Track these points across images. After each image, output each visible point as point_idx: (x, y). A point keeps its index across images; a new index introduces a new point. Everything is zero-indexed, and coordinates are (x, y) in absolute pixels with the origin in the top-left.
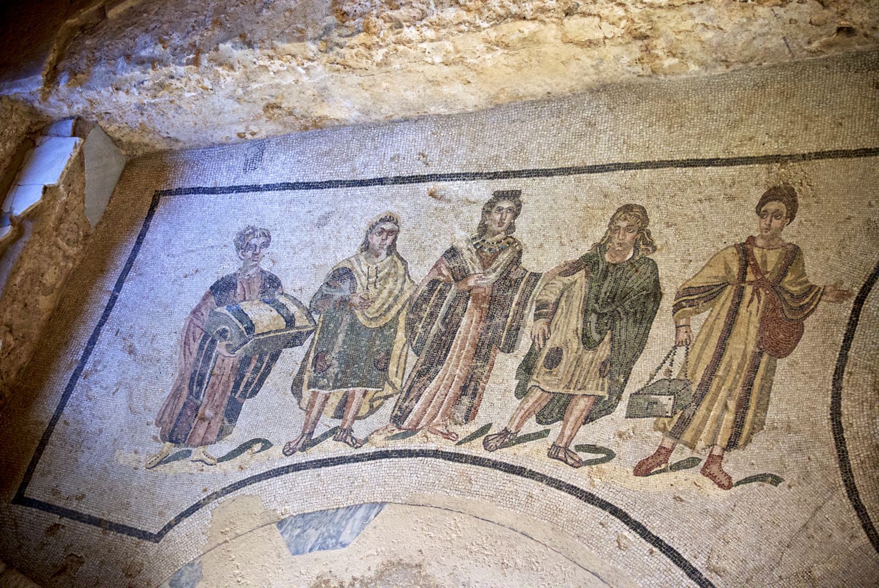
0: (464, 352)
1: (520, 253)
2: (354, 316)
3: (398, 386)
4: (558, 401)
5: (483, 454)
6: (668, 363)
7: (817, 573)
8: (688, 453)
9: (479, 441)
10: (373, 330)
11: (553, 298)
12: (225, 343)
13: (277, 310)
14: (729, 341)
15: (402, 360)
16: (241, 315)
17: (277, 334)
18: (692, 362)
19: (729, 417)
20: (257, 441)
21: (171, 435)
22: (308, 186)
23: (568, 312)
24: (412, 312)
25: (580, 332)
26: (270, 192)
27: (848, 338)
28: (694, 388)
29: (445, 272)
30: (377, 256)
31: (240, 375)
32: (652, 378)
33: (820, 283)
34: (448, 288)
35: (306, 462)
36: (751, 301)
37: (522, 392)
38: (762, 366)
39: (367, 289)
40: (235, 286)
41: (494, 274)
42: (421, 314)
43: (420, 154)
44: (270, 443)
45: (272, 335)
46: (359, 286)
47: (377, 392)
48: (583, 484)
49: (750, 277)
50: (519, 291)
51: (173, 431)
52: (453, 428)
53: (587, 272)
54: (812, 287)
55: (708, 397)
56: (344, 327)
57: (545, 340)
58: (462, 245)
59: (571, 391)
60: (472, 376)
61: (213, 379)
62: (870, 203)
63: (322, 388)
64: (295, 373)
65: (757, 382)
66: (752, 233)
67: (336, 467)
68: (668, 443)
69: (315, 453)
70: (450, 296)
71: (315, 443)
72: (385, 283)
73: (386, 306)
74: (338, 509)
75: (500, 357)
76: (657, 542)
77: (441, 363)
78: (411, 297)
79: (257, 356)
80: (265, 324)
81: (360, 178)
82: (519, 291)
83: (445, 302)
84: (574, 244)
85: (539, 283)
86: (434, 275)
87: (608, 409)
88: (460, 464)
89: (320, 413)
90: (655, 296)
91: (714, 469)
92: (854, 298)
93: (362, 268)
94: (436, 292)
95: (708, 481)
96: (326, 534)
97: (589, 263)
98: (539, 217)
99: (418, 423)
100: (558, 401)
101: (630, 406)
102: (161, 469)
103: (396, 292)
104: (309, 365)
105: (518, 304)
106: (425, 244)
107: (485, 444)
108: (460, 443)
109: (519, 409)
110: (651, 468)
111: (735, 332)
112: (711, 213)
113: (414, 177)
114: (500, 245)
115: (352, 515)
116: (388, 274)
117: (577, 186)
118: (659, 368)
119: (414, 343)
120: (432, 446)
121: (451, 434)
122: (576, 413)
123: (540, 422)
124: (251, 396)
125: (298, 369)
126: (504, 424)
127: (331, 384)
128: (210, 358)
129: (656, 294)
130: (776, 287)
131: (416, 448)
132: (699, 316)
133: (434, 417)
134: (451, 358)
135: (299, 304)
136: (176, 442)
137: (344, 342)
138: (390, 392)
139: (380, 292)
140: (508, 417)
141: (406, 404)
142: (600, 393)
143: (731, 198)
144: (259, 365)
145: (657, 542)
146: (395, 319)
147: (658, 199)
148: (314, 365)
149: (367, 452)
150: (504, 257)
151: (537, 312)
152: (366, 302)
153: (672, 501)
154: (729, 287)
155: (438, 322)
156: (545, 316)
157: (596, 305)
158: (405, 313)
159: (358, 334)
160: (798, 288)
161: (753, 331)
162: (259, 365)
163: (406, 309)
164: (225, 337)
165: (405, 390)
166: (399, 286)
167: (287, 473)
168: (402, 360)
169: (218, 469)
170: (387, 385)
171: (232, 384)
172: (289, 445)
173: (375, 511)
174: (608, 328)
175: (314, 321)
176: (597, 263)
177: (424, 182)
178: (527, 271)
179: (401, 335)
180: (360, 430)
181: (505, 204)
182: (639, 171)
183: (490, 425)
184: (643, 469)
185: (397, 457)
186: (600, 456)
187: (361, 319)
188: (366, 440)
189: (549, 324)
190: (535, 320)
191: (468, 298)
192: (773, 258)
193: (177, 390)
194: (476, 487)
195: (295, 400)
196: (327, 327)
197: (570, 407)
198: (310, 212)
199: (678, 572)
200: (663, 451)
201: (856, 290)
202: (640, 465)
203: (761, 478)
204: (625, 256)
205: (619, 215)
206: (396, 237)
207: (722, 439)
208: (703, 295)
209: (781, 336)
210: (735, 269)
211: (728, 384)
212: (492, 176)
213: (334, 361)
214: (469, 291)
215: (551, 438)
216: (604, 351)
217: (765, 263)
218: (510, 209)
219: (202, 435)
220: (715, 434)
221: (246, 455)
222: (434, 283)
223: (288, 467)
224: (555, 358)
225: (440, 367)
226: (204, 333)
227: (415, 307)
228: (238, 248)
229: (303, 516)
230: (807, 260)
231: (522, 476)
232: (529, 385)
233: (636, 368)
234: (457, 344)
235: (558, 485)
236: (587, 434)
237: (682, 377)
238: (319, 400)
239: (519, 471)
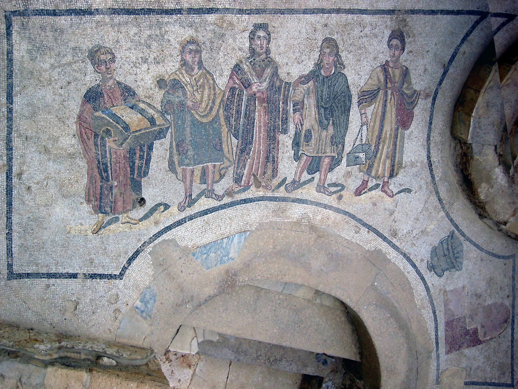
0: (262, 135)
1: (277, 68)
2: (192, 115)
3: (232, 160)
4: (315, 161)
5: (287, 195)
6: (360, 136)
8: (375, 182)
9: (282, 188)
12: (112, 139)
13: (141, 114)
16: (114, 116)
17: (146, 131)
20: (160, 204)
28: (373, 148)
30: (193, 70)
34: (242, 93)
35: (194, 214)
36: (391, 99)
37: (297, 158)
39: (194, 94)
40: (101, 95)
41: (265, 83)
44: (168, 205)
45: (143, 132)
46: (188, 93)
47: (221, 165)
49: (389, 85)
53: (314, 82)
55: (380, 152)
57: (302, 125)
60: (270, 150)
63: (188, 165)
64: (168, 157)
65: (398, 143)
67: (212, 214)
69: (197, 208)
74: (222, 239)
75: (281, 137)
79: (139, 148)
82: (282, 94)
83: (243, 103)
85: (291, 89)
86: (231, 84)
88: (277, 203)
89: (191, 182)
91: (386, 188)
92: (432, 97)
94: (236, 96)
96: (221, 255)
97: (313, 75)
99: (249, 182)
100: (315, 161)
101: (347, 160)
103: (212, 97)
104: (175, 151)
108: (273, 191)
109: (298, 167)
110: (361, 191)
115: (232, 242)
116: (203, 83)
118: (357, 138)
120: (261, 194)
122: (325, 166)
123: (309, 174)
124: (145, 176)
125: (168, 154)
127: (192, 163)
131: (252, 197)
134: (256, 140)
135: (154, 108)
137: (191, 133)
139: (202, 97)
140: (294, 173)
142: (333, 154)
144: (142, 153)
146: (217, 115)
149: (227, 202)
150: (268, 71)
151: (294, 108)
152: (197, 105)
154: (381, 91)
156: (299, 110)
157: (322, 103)
158: (222, 111)
161: (394, 116)
162: (142, 153)
164: (110, 135)
165: (236, 162)
167: (186, 222)
168: (229, 141)
170: (225, 160)
171: (129, 169)
172: (180, 205)
174: (330, 116)
175: (168, 120)
176: (318, 76)
178: (283, 81)
183: (286, 178)
184: (358, 192)
185: (244, 204)
186: (339, 188)
187: (197, 117)
189: (301, 115)
190: (294, 113)
197: (321, 163)
202: (357, 190)
204: (331, 72)
208: (370, 96)
209: (405, 119)
214: (255, 95)
215: (316, 181)
216: (331, 130)
222: (233, 89)
223: (185, 218)
224: (308, 136)
225: (251, 146)
226: (93, 133)
231: (307, 204)
232: (301, 152)
234: (256, 130)
235: (326, 207)
236: (332, 177)
237: (367, 143)
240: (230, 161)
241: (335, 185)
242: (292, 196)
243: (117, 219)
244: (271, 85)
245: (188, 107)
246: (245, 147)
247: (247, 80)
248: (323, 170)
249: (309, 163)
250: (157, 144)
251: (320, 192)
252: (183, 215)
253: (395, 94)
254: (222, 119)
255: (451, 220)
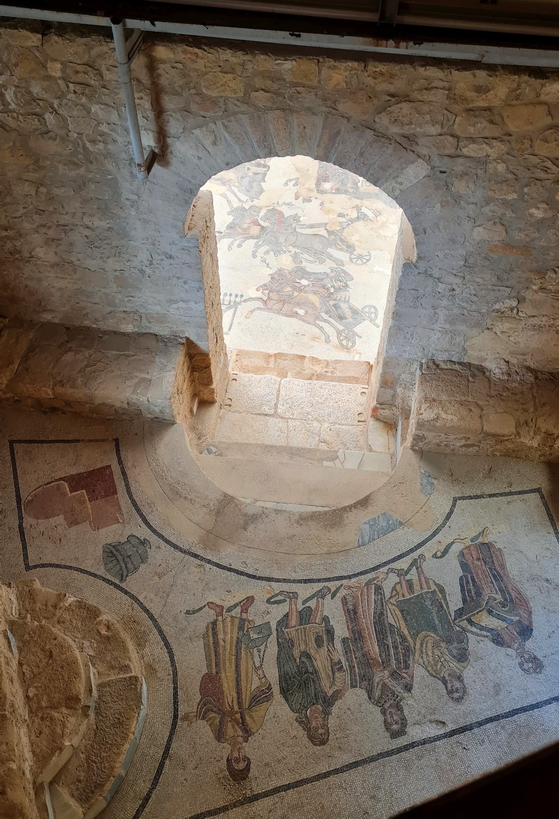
0: (367, 632)
1: (370, 698)
2: (438, 635)
3: (390, 605)
5: (327, 584)
7: (156, 578)
8: (233, 613)
9: (333, 590)
10: (422, 631)
11: (337, 675)
14: (236, 676)
15: (396, 620)
16: (504, 619)
18: (250, 659)
19: (221, 636)
20: (441, 557)
21: (488, 547)
22: (524, 710)
23: (325, 669)
24: (408, 646)
25: (313, 660)
26: (545, 699)
27: (176, 694)
29: (405, 675)
30: (449, 674)
31: (476, 586)
32: (266, 645)
33: (200, 722)
34: (397, 666)
37: (326, 619)
38: (214, 667)
40: (520, 634)
42: (402, 647)
43: (469, 749)
45: (475, 612)
46: (447, 653)
47: (398, 598)
48: (274, 584)
49: (238, 716)
50: (357, 674)
51: (489, 549)
52: (350, 592)
54: (203, 718)
56: (439, 626)
58: (406, 695)
59: (302, 627)
61: (489, 580)
62: (187, 782)
63: (428, 592)
64: (447, 596)
65: (213, 657)
66: (247, 744)
68: (244, 616)
70: (393, 662)
71: (412, 565)
72: (434, 660)
73: (424, 646)
75: (347, 634)
76: (230, 570)
77: (374, 623)
78: (414, 654)
80: (483, 617)
81: (495, 723)
82: (357, 674)
84: (342, 712)
86: (410, 671)
87: (279, 623)
89: (420, 580)
90: (283, 690)
91: (218, 610)
93: (454, 665)
94: (402, 662)
95: (219, 603)
98: (371, 724)
101: (270, 628)
102: (481, 530)
104: (443, 602)
105: (354, 667)
106: (427, 690)
107: (329, 590)
108: (341, 585)
110: (247, 601)
111: (235, 681)
112: (275, 752)
113: (462, 732)
114: (384, 700)
116: (436, 666)
117: (359, 750)
118: (264, 651)
119: (396, 630)
120: (353, 580)
121: (348, 589)
123: (309, 607)
124: (461, 577)
125: (448, 598)
126: (326, 601)
128: (500, 590)
129: (284, 692)
130: (223, 714)
132: (256, 686)
133: (361, 595)
134: (372, 627)
135: (473, 633)
136: (483, 544)
138: (391, 600)
139: (433, 653)
140: (326, 605)
141: (380, 597)
143: (267, 765)
145: (230, 570)
147: (308, 753)
148: (440, 603)
150: (377, 693)
152: (436, 645)
153: (231, 590)
154: (247, 707)
155: (391, 645)
156: (336, 664)
159: (429, 626)
160: (211, 716)
161: (225, 685)
163: (412, 647)
165: (385, 604)
166: (425, 659)
168: (396, 620)
169: (451, 538)
170: (395, 603)
171: (476, 580)
173: (360, 542)
176: (324, 702)
177: (453, 730)
179: (406, 632)
180: (394, 578)
181: (395, 727)
182: (328, 770)
183: (332, 599)
184: (250, 600)
186: (272, 600)
187: (433, 635)
188: (387, 573)
189: (331, 660)
190: (340, 660)
191: (383, 663)
192: (230, 730)
193: (504, 569)
194: (322, 567)
195: (436, 581)
196: (448, 625)
198: (510, 692)
199: (215, 560)
200: (245, 611)
201: (179, 723)
202: (252, 602)
203: (195, 612)
204: (311, 711)
205: (326, 737)
206: (446, 689)
207: (220, 625)
208: (259, 699)
210: (247, 718)
211: (227, 653)
212: (414, 745)
213: (431, 608)
214: (384, 667)
215: (300, 602)
217: (233, 727)
218: (391, 725)
219: (472, 552)
220: (224, 627)
221: (442, 548)
222: (407, 667)
224: (319, 642)
227: (408, 651)
228: (535, 658)
229: (393, 530)
230: (211, 734)
233: (276, 648)
235: (285, 581)
236: (284, 608)
237: (251, 650)
238: (425, 586)
239: (306, 581)
240: (391, 603)
241: (278, 602)
242: (322, 585)
243: (472, 540)
244: (370, 680)
245: (444, 641)
246: (379, 618)
247: (396, 679)
248: (295, 613)
249: (312, 617)
250: (460, 605)
251: (293, 593)
252: (419, 552)
253: (228, 708)
254: (409, 639)
255: (126, 593)
